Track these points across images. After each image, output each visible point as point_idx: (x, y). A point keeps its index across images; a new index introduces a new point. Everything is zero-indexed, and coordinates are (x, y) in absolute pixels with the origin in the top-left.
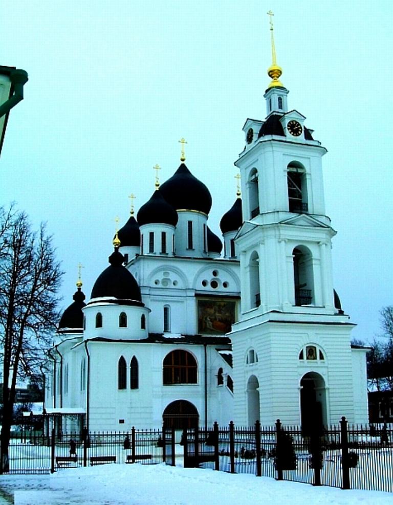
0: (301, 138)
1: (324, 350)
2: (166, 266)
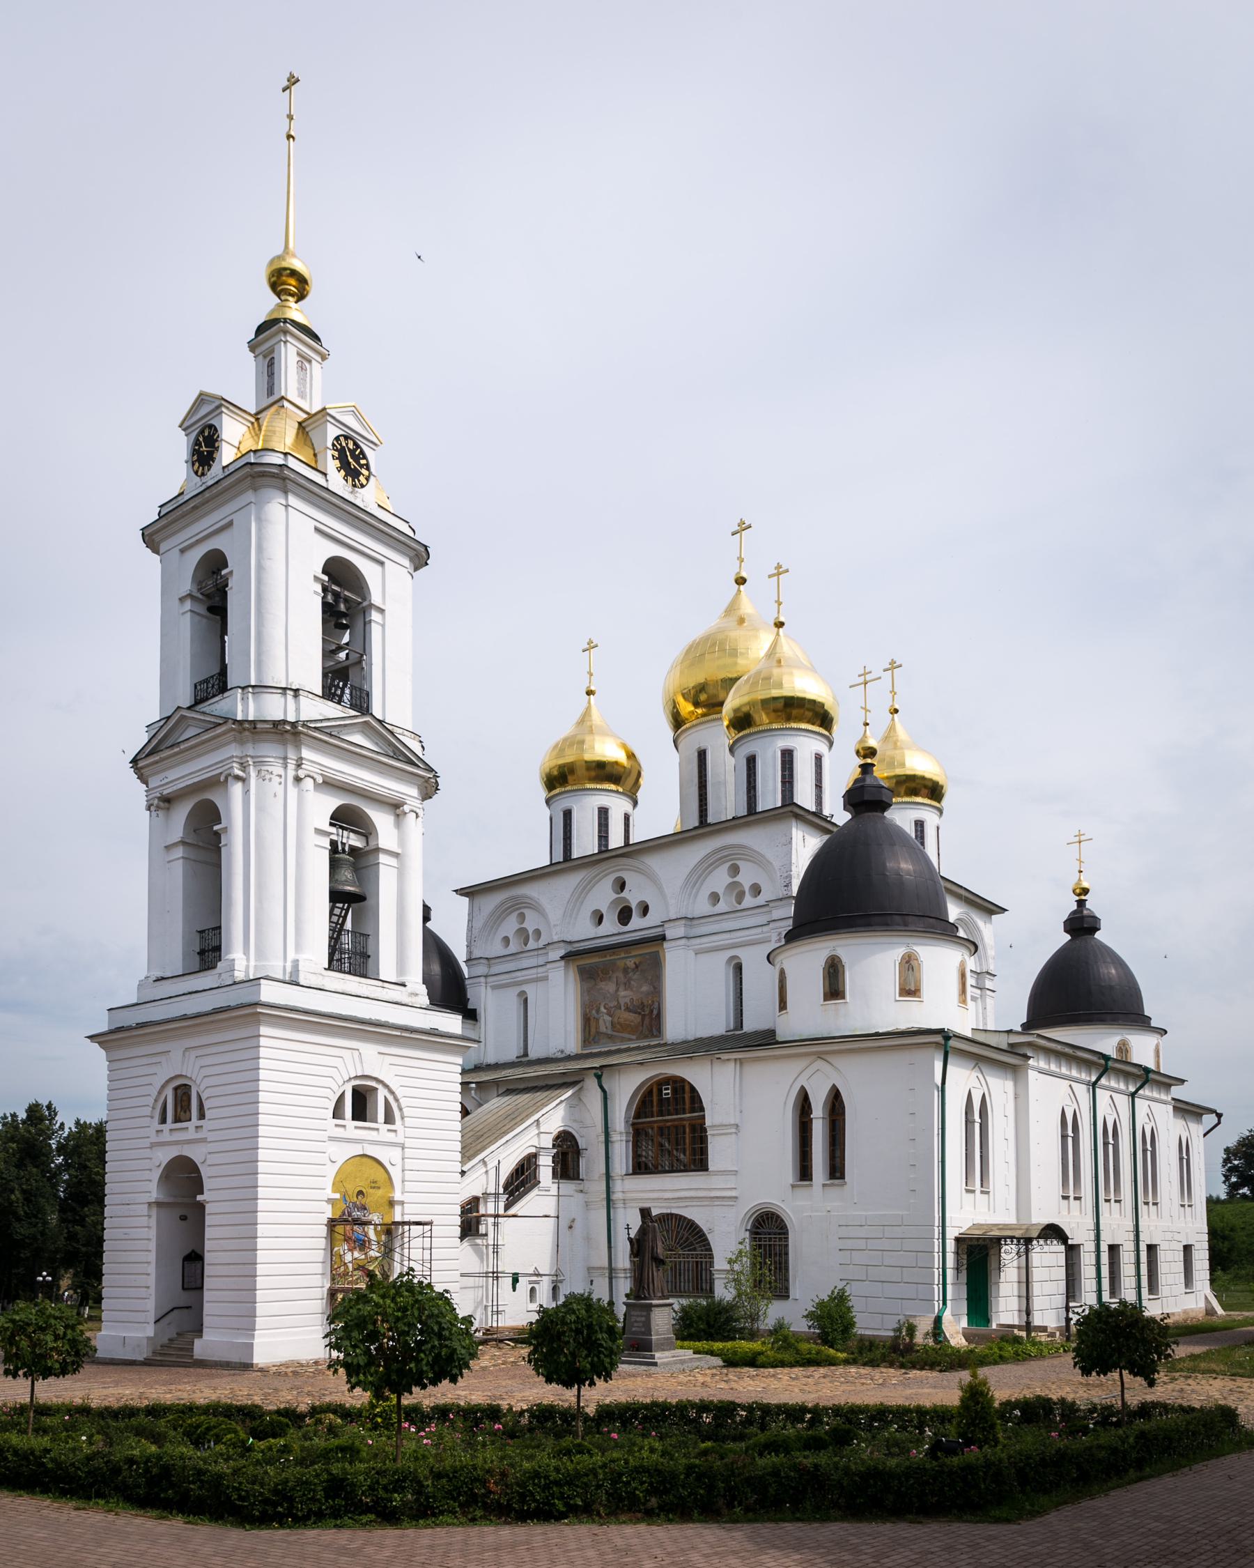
1: (397, 1100)
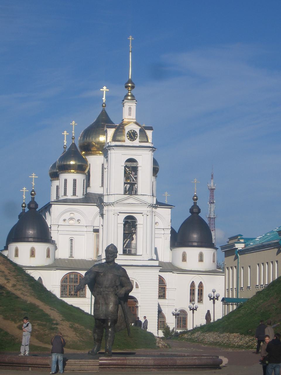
0: (137, 142)
2: (71, 208)
